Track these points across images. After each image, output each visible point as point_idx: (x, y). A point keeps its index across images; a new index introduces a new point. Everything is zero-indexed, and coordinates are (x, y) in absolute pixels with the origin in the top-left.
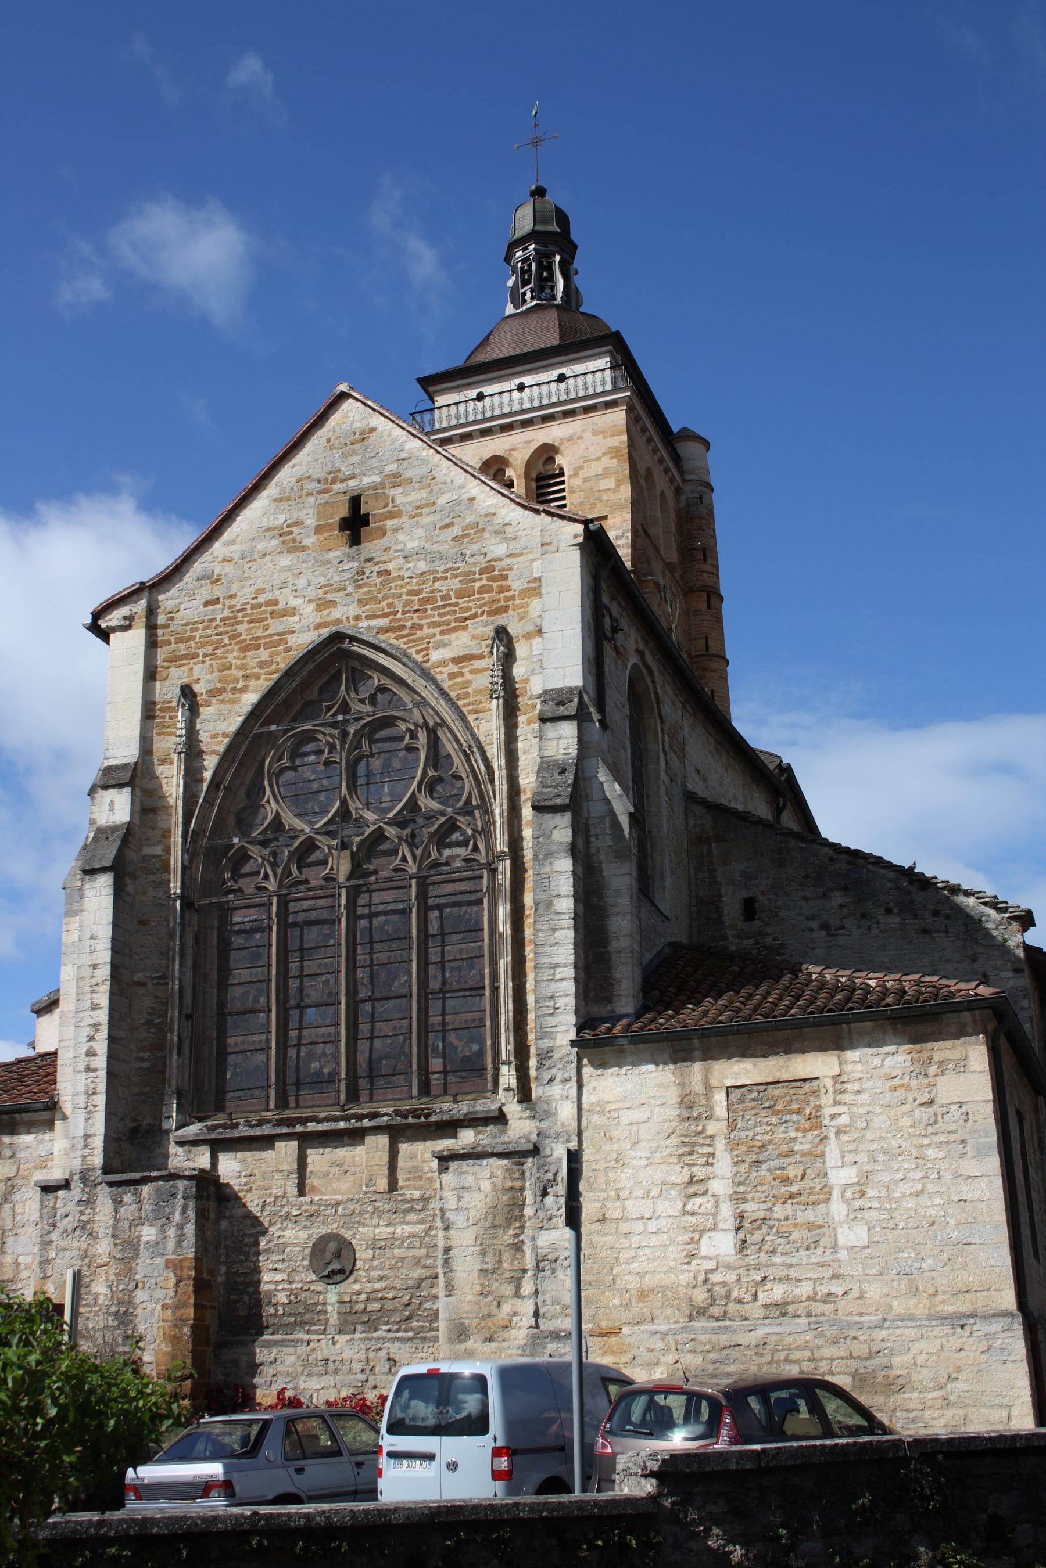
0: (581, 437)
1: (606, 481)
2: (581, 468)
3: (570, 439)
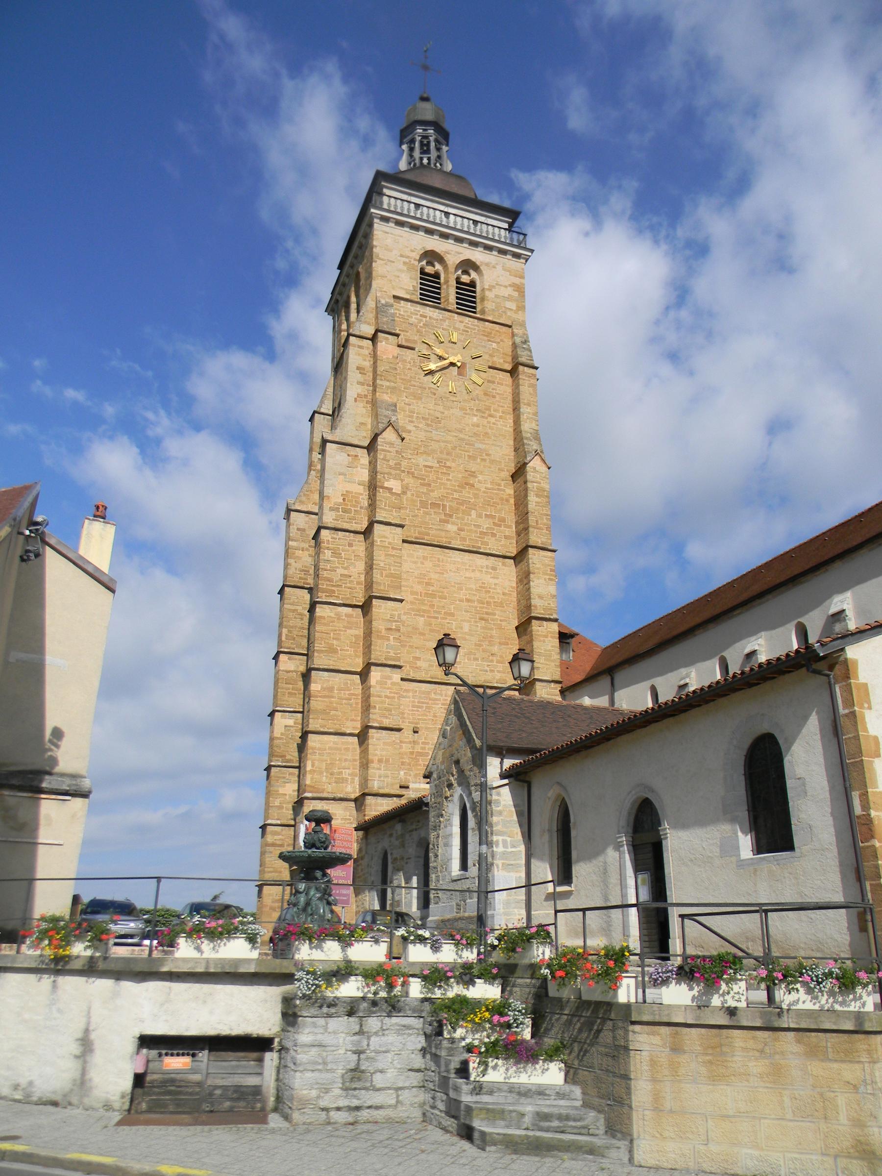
0: (494, 267)
1: (510, 303)
2: (493, 287)
3: (487, 264)
